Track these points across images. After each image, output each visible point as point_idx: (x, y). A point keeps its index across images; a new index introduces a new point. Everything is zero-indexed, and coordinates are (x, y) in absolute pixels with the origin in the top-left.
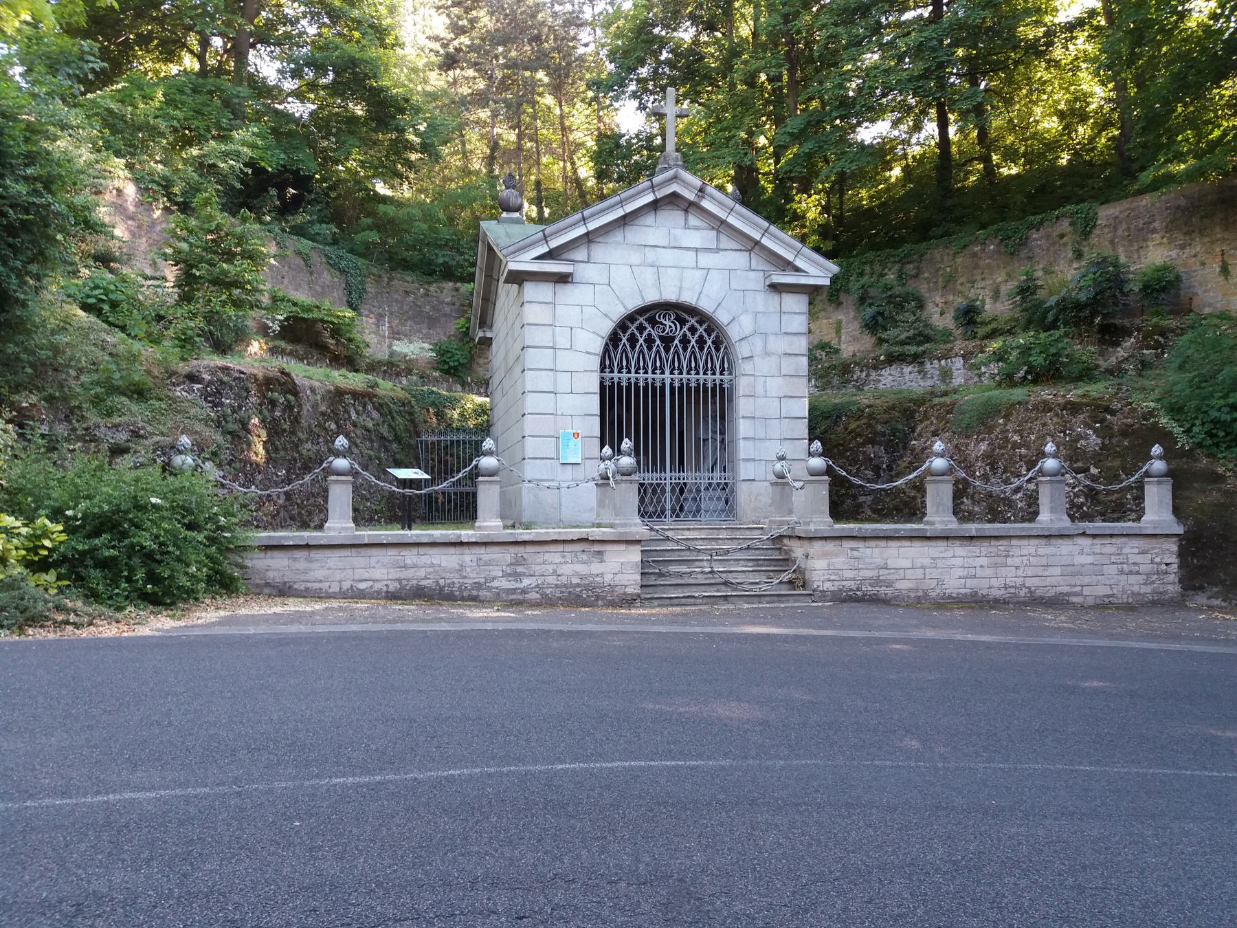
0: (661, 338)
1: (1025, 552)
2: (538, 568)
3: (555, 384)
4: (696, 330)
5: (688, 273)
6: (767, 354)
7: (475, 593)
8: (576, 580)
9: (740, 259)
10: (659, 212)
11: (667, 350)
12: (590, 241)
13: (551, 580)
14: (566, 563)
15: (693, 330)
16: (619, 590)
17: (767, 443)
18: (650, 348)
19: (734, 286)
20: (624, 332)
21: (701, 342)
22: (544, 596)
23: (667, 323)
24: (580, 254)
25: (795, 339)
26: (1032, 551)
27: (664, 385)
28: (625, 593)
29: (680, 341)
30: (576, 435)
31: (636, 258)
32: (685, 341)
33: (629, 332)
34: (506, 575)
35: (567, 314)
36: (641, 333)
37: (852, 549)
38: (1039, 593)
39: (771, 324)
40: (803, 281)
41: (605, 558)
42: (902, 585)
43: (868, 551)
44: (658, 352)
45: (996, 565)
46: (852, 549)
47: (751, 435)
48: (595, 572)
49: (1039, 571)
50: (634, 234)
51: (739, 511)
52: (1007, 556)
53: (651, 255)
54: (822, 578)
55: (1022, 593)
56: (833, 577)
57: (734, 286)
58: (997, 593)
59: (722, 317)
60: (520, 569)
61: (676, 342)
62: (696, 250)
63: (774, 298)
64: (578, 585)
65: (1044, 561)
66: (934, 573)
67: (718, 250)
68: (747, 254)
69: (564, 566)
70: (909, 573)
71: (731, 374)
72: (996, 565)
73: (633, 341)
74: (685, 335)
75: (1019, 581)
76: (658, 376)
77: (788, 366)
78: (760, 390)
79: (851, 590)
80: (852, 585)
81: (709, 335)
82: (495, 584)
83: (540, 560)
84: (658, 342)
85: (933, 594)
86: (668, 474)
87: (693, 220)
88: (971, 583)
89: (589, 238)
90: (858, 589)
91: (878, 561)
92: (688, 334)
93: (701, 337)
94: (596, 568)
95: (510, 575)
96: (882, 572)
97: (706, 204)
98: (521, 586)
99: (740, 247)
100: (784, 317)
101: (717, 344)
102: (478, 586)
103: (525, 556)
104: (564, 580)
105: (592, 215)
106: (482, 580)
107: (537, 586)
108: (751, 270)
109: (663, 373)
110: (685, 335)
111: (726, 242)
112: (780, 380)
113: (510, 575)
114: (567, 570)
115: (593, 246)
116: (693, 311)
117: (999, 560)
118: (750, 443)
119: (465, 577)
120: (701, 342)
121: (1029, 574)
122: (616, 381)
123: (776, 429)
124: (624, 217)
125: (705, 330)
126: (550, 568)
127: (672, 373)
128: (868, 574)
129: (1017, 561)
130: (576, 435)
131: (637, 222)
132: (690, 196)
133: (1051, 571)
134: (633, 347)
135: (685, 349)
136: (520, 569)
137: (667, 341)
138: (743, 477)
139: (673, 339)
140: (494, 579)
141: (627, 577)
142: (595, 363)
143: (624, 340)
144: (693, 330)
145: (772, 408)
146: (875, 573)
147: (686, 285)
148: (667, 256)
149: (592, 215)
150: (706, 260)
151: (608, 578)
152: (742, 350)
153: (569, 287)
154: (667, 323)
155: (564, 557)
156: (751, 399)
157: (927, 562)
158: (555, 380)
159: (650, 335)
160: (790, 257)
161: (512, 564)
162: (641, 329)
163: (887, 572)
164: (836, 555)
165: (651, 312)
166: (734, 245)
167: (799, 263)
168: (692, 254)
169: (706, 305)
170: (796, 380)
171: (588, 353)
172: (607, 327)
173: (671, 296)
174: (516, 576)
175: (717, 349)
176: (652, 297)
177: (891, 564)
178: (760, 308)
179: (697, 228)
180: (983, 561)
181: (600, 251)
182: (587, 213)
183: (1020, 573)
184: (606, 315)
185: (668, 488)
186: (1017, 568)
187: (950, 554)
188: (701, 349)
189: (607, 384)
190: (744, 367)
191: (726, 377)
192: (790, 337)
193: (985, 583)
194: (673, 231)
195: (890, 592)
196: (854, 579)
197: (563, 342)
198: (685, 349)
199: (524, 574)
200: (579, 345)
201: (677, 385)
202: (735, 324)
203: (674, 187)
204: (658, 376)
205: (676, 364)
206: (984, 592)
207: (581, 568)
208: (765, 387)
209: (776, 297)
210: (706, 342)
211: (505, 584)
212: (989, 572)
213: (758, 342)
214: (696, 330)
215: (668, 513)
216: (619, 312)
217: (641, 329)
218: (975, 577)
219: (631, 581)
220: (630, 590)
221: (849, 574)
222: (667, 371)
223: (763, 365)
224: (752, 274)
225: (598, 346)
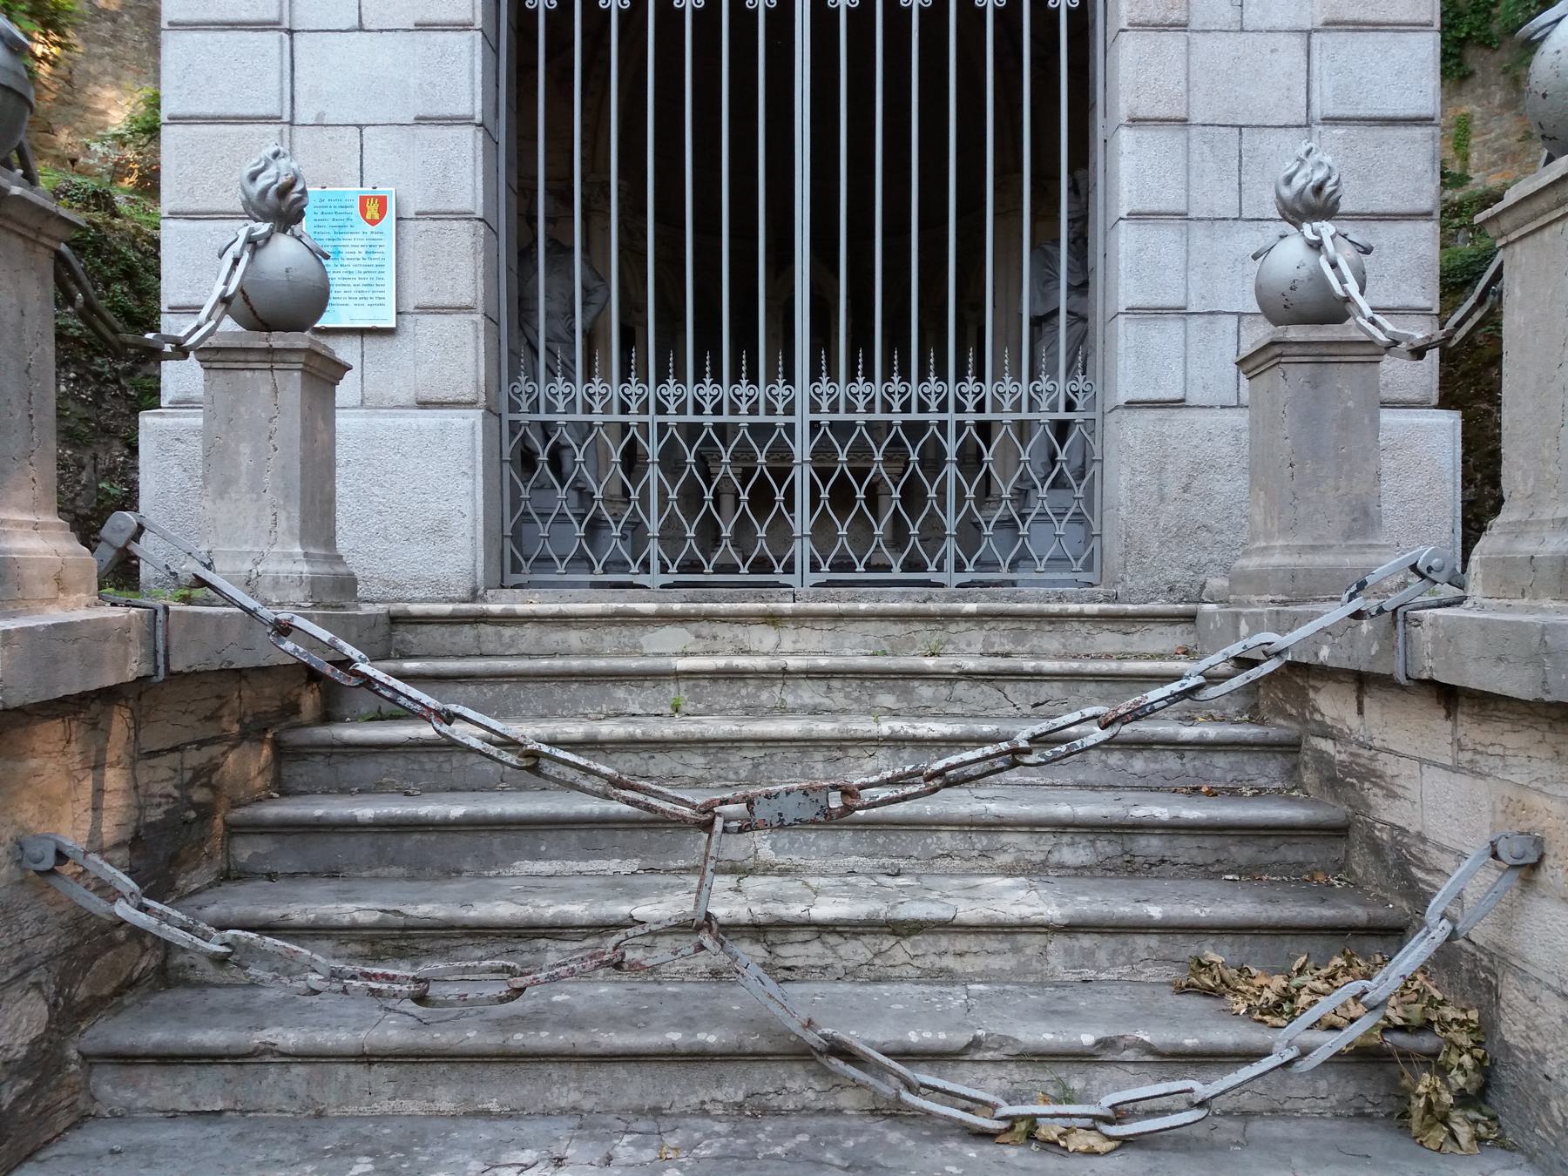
30: (373, 207)
47: (1171, 200)
51: (1113, 547)
118: (1166, 238)
130: (373, 207)
138: (1126, 385)
156: (1173, 42)
215: (802, 550)
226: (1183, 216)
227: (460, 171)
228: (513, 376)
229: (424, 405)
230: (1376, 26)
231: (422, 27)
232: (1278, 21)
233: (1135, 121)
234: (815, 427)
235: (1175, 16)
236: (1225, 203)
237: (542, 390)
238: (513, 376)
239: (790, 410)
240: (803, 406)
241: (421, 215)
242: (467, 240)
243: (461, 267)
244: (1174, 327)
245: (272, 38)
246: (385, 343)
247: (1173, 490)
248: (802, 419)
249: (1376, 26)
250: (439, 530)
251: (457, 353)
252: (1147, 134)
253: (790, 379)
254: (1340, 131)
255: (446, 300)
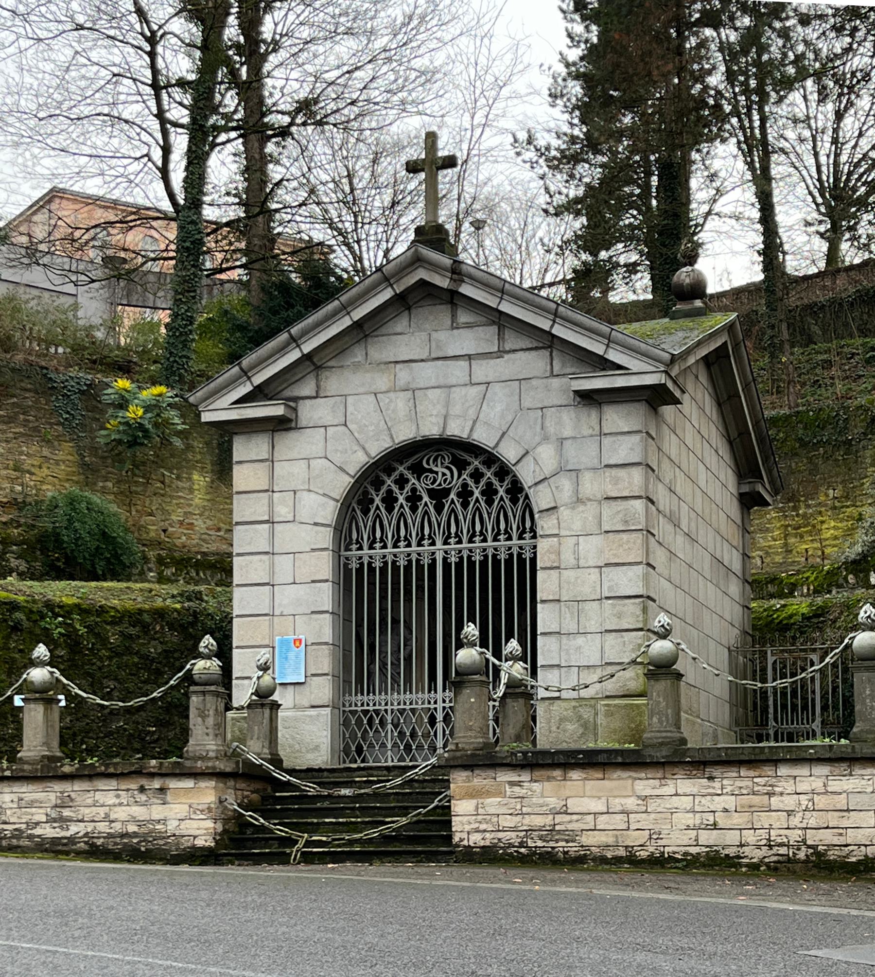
0: (431, 493)
1: (803, 787)
2: (87, 811)
3: (272, 573)
4: (482, 475)
5: (457, 394)
6: (579, 501)
7: (14, 842)
8: (132, 828)
9: (534, 363)
10: (413, 311)
11: (439, 509)
12: (318, 368)
13: (103, 827)
14: (121, 804)
15: (477, 476)
16: (186, 843)
17: (580, 640)
18: (414, 509)
19: (526, 403)
20: (378, 490)
21: (489, 493)
22: (93, 845)
23: (440, 469)
24: (307, 388)
25: (622, 473)
26: (818, 784)
27: (434, 561)
28: (194, 847)
29: (459, 495)
31: (382, 382)
32: (465, 494)
33: (384, 489)
34: (50, 820)
35: (291, 472)
36: (402, 488)
37: (512, 784)
38: (832, 855)
39: (583, 454)
40: (621, 382)
41: (169, 798)
42: (590, 840)
43: (536, 786)
44: (426, 513)
45: (751, 809)
46: (512, 784)
47: (554, 628)
48: (156, 817)
49: (833, 819)
50: (385, 349)
52: (770, 794)
53: (403, 374)
54: (467, 828)
55: (801, 855)
56: (483, 827)
57: (526, 403)
58: (755, 855)
59: (509, 453)
60: (66, 813)
61: (452, 496)
62: (469, 357)
63: (589, 419)
64: (135, 835)
65: (841, 802)
66: (646, 822)
67: (500, 353)
68: (546, 353)
69: (116, 809)
70: (603, 821)
71: (534, 537)
72: (751, 809)
73: (390, 501)
74: (465, 485)
75: (795, 836)
76: (427, 548)
77: (611, 515)
78: (568, 557)
79: (511, 845)
80: (513, 837)
81: (502, 481)
82: (38, 831)
83: (89, 801)
84: (426, 499)
85: (644, 854)
86: (440, 695)
87: (464, 317)
88: (708, 838)
89: (313, 363)
90: (521, 845)
91: (553, 802)
92: (470, 482)
93: (489, 484)
94: (157, 811)
95: (55, 820)
96: (559, 818)
97: (466, 290)
98: (68, 834)
99: (535, 344)
100: (606, 441)
101: (516, 490)
102: (18, 834)
103: (73, 795)
104: (117, 827)
105: (305, 333)
106: (24, 826)
107: (86, 834)
108: (552, 375)
109: (433, 544)
110: (465, 485)
111: (512, 341)
112: (596, 541)
113: (55, 820)
114: (120, 814)
115: (324, 374)
116: (474, 449)
117: (756, 800)
119: (5, 823)
120: (489, 493)
121: (812, 823)
122: (366, 561)
123: (596, 617)
124: (358, 325)
125: (496, 474)
126: (102, 811)
127: (446, 543)
128: (538, 821)
129: (789, 802)
131: (383, 330)
132: (443, 282)
133: (854, 819)
134: (390, 509)
135: (465, 505)
136: (66, 813)
137: (439, 495)
139: (447, 492)
140: (37, 824)
141: (195, 824)
142: (326, 538)
143: (377, 501)
144: (477, 476)
145: (587, 583)
146: (548, 820)
147: (456, 410)
148: (427, 373)
149: (305, 333)
150: (483, 370)
151: (172, 826)
152: (540, 499)
153: (293, 435)
154: (440, 469)
155: (118, 796)
157: (631, 803)
158: (272, 565)
159: (414, 490)
160: (598, 348)
161: (56, 806)
162: (401, 482)
163: (567, 818)
164: (489, 794)
165: (413, 454)
166: (527, 343)
167: (614, 356)
168: (464, 364)
169: (484, 437)
170: (625, 536)
171: (316, 524)
172: (342, 484)
173: (431, 429)
174: (63, 821)
175: (514, 501)
176: (405, 434)
177: (574, 805)
178: (568, 432)
179: (469, 326)
180: (730, 802)
181: (333, 382)
182: (295, 330)
183: (795, 821)
184: (341, 469)
185: (440, 716)
186: (790, 813)
187: (669, 789)
188: (490, 502)
189: (354, 566)
190: (545, 525)
191: (527, 541)
192: (614, 472)
193: (732, 838)
194: (434, 335)
195: (573, 849)
196: (514, 829)
197: (283, 511)
198: (465, 505)
199: (69, 820)
200: (304, 514)
201: (453, 560)
202: (529, 459)
203: (421, 274)
204: (427, 548)
205: (453, 529)
206: (731, 851)
207: (139, 812)
208: (576, 553)
209: (594, 414)
210: (496, 492)
211: (49, 832)
212: (738, 820)
213: (566, 484)
214: (482, 475)
216: (358, 461)
217: (401, 482)
218: (715, 826)
219: (202, 831)
220: (200, 843)
221: (508, 822)
222: (439, 544)
223: (572, 520)
224: (556, 382)
225: (329, 512)
226: (559, 633)
227: (325, 629)
228: (344, 695)
229: (313, 707)
230: (623, 564)
231: (313, 582)
232: (591, 563)
233: (543, 601)
234: (444, 708)
235: (555, 565)
236: (573, 628)
237: (353, 699)
238: (344, 695)
239: (435, 703)
240: (440, 701)
241: (313, 644)
242: (327, 652)
243: (324, 661)
244: (556, 671)
245: (268, 587)
246: (302, 687)
247: (554, 729)
248: (440, 705)
249: (623, 564)
250: (317, 748)
251: (323, 690)
252: (546, 605)
253: (436, 692)
254: (610, 602)
255: (320, 672)
